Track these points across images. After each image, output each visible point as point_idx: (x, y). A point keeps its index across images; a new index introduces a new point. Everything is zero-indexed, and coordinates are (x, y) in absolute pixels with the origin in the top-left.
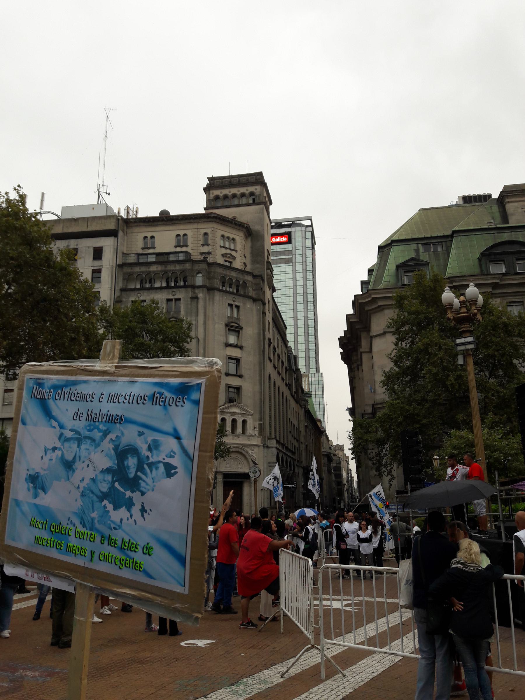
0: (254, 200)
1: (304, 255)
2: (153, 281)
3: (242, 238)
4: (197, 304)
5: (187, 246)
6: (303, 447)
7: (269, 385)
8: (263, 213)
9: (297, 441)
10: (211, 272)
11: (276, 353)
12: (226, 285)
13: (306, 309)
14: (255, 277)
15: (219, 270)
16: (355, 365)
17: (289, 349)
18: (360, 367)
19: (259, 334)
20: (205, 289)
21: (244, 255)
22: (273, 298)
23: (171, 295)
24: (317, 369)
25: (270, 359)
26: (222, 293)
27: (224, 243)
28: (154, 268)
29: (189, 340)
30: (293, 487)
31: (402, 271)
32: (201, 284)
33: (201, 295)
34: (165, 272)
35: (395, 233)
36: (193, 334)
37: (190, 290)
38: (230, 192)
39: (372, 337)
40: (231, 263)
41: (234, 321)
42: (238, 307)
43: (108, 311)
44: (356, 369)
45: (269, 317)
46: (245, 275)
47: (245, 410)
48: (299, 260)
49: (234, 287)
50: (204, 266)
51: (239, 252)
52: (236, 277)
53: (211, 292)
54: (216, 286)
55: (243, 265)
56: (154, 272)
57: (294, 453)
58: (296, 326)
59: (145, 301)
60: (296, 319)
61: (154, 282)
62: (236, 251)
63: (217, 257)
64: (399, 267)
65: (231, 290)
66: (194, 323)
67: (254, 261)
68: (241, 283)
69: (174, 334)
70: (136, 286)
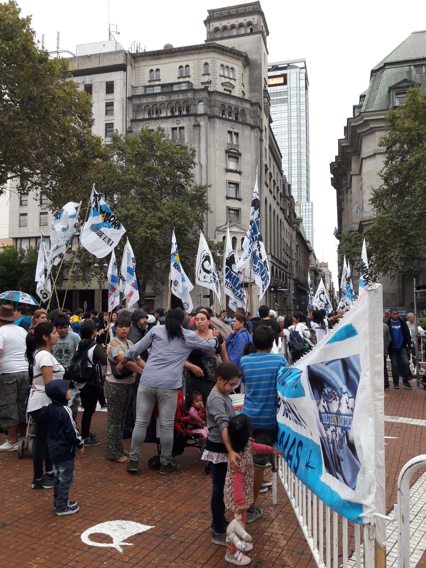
0: (251, 29)
1: (298, 95)
2: (159, 111)
3: (240, 67)
4: (199, 131)
5: (189, 77)
6: (294, 263)
7: (266, 208)
8: (260, 42)
9: (290, 257)
10: (212, 100)
11: (272, 179)
12: (226, 112)
13: (299, 145)
14: (252, 104)
15: (219, 98)
16: (344, 188)
17: (284, 179)
18: (349, 190)
19: (257, 160)
20: (206, 117)
21: (243, 84)
22: (270, 127)
23: (175, 124)
24: (308, 200)
25: (266, 184)
26: (222, 120)
27: (224, 73)
28: (159, 99)
29: (193, 165)
30: (286, 291)
31: (393, 93)
32: (202, 112)
33: (202, 123)
34: (170, 102)
35: (388, 56)
36: (196, 160)
37: (192, 118)
38: (229, 23)
39: (362, 159)
40: (230, 91)
41: (233, 148)
42: (237, 134)
43: (120, 139)
44: (345, 192)
45: (266, 144)
46: (244, 103)
47: (244, 229)
48: (294, 100)
49: (233, 115)
50: (204, 95)
51: (238, 81)
52: (235, 105)
53: (212, 120)
54: (217, 114)
55: (242, 94)
56: (160, 102)
57: (286, 267)
58: (290, 154)
59: (152, 130)
60: (290, 146)
61: (161, 113)
62: (235, 80)
63: (217, 86)
64: (391, 89)
65: (230, 118)
66: (197, 149)
67: (252, 90)
68: (239, 111)
69: (179, 160)
70: (144, 116)
